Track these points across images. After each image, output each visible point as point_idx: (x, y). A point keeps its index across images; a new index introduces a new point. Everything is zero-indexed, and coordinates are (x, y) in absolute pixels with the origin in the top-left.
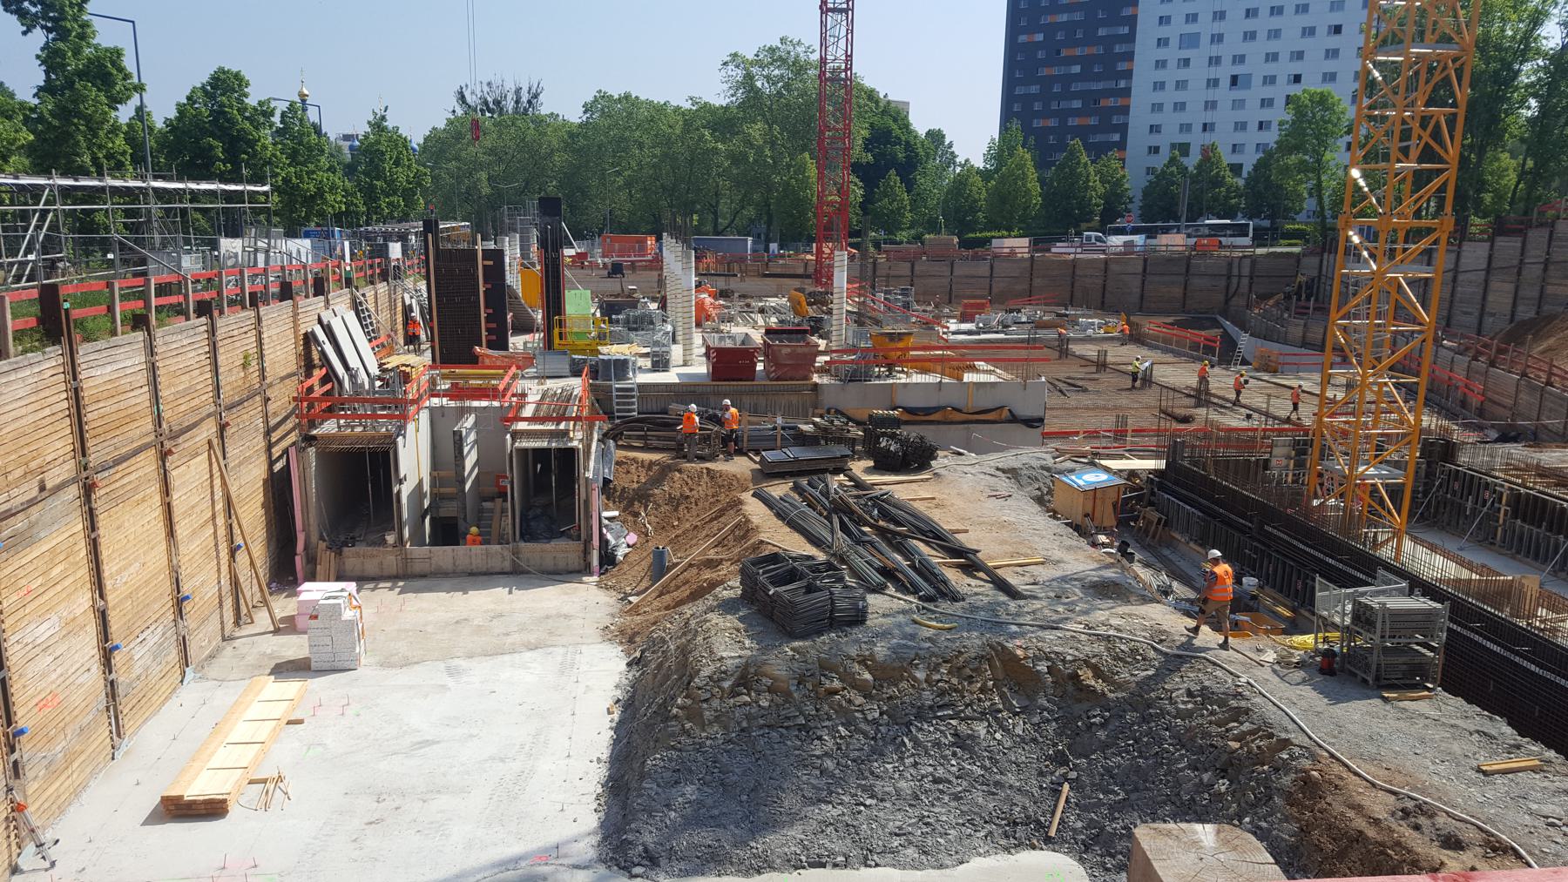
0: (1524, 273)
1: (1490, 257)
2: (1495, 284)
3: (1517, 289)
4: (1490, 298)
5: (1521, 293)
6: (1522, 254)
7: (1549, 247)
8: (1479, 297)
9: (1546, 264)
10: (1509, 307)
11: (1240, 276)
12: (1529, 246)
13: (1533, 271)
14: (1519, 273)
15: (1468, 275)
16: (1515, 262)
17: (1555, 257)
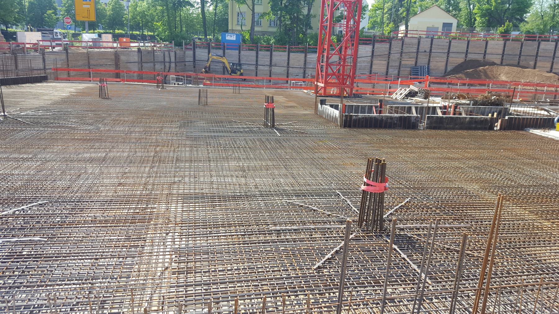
0: (391, 56)
1: (373, 51)
2: (374, 62)
3: (388, 63)
4: (374, 67)
5: (390, 64)
6: (390, 49)
7: (402, 47)
8: (369, 67)
9: (401, 53)
10: (385, 70)
11: (170, 62)
12: (392, 47)
13: (395, 56)
14: (389, 58)
15: (363, 59)
16: (387, 53)
17: (405, 51)
